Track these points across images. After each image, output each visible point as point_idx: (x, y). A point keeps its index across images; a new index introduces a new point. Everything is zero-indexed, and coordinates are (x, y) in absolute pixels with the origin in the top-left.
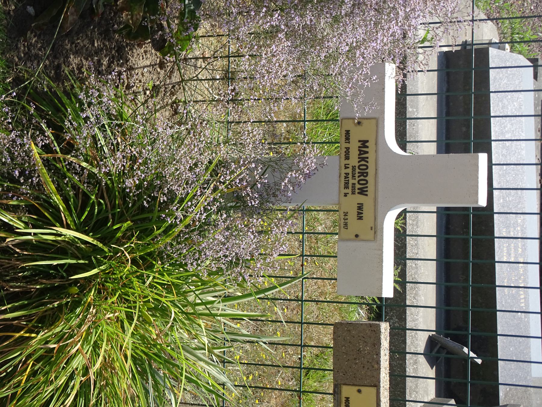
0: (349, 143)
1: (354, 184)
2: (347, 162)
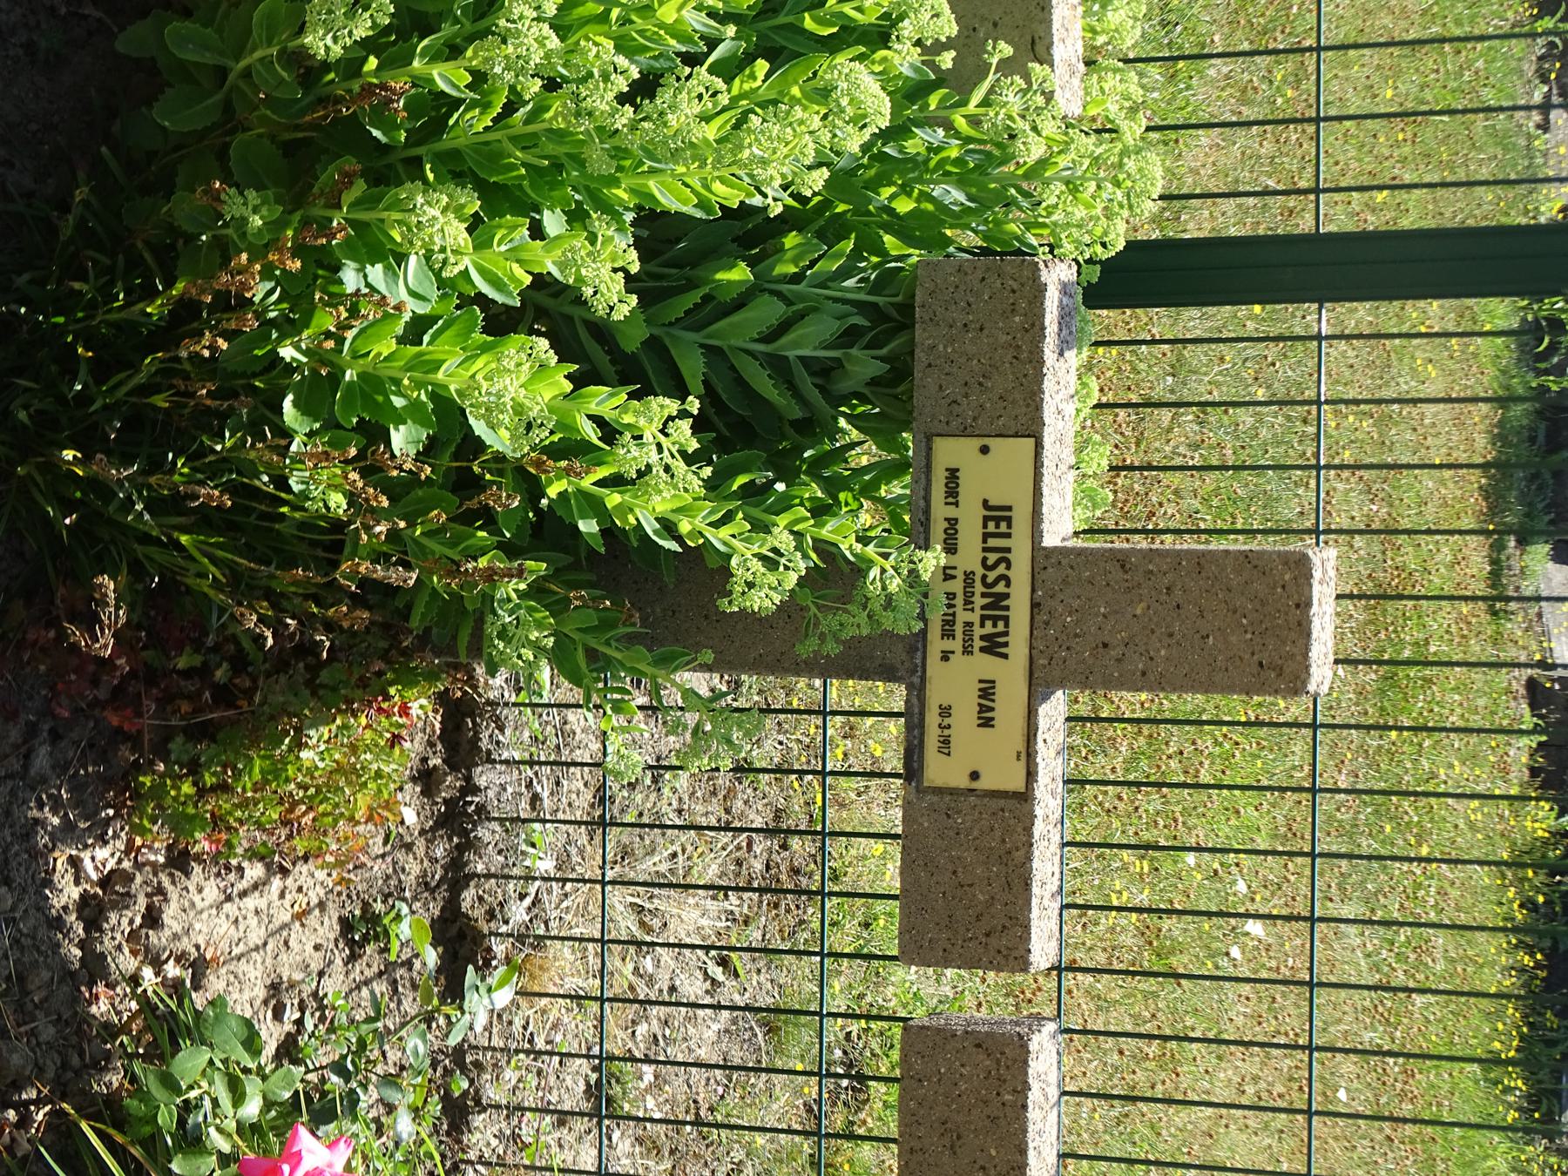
1: (969, 624)
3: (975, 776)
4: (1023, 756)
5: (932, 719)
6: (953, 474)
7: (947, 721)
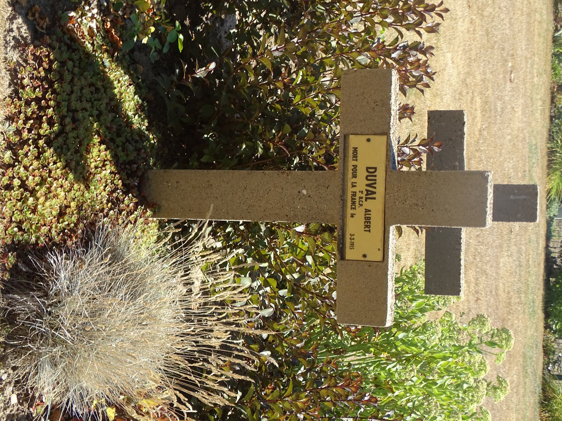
0: (357, 160)
2: (354, 180)
3: (365, 256)
4: (382, 249)
5: (348, 237)
6: (355, 149)
7: (353, 237)
